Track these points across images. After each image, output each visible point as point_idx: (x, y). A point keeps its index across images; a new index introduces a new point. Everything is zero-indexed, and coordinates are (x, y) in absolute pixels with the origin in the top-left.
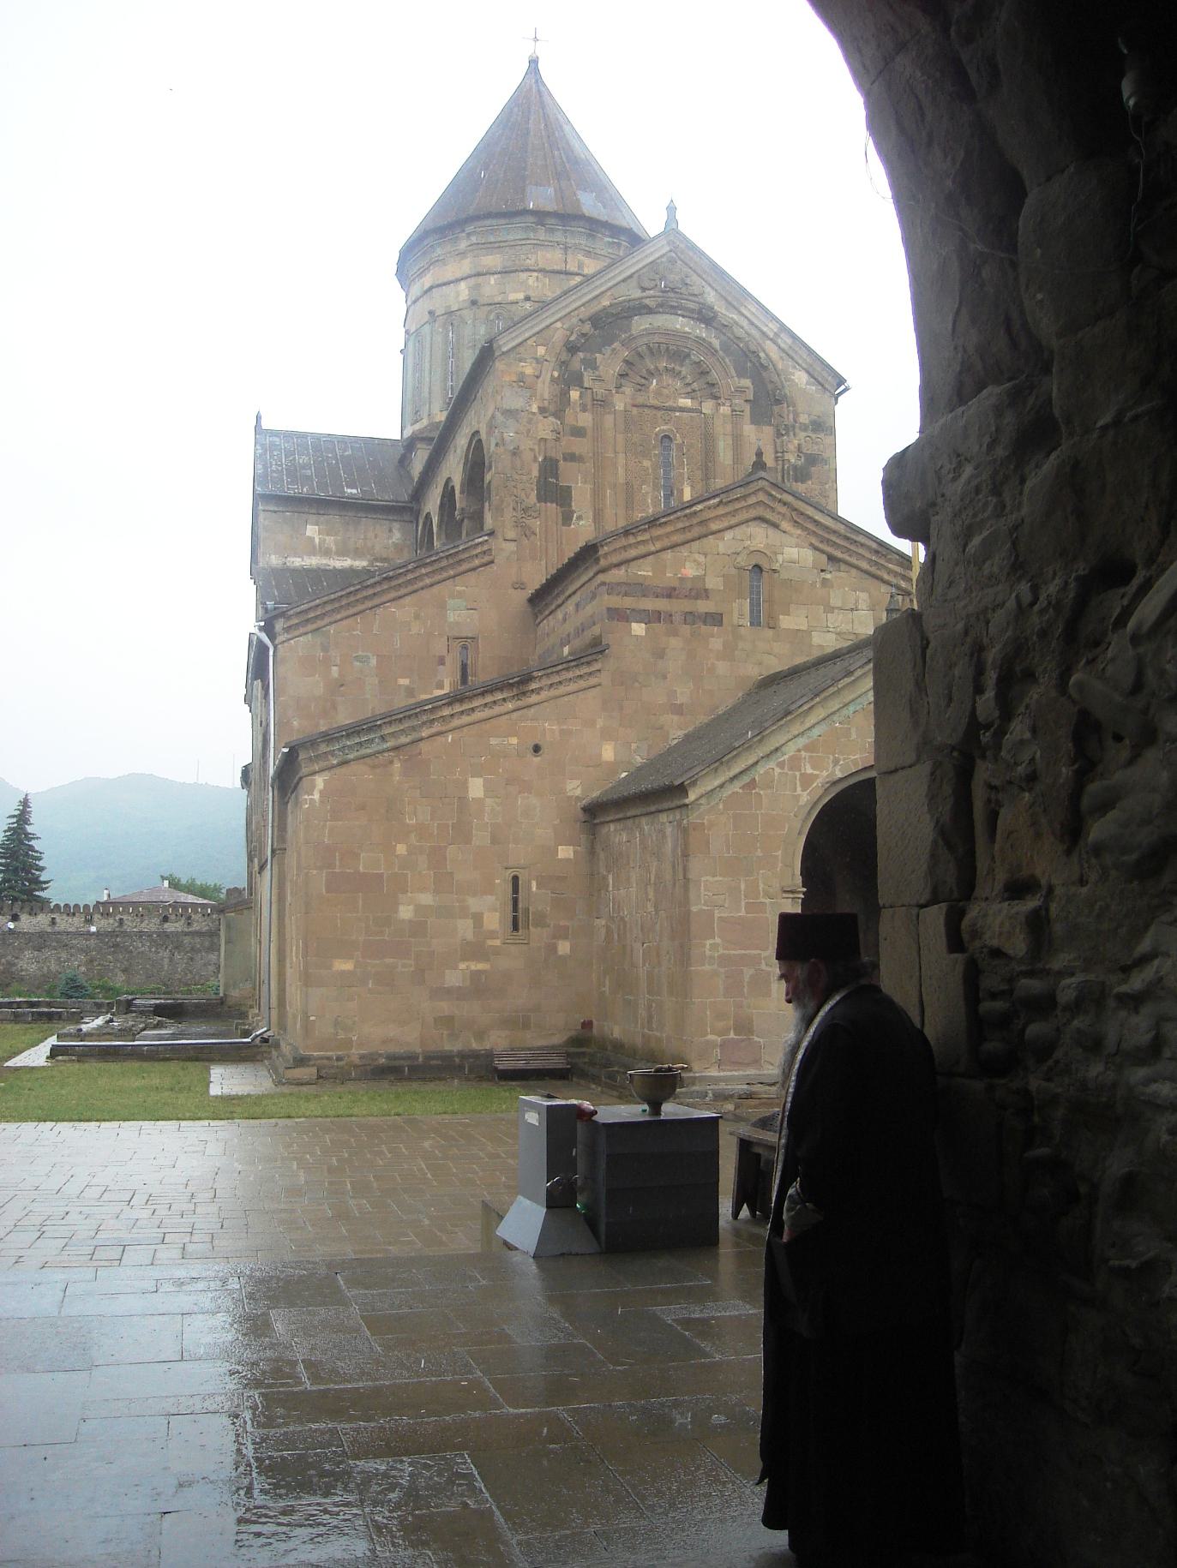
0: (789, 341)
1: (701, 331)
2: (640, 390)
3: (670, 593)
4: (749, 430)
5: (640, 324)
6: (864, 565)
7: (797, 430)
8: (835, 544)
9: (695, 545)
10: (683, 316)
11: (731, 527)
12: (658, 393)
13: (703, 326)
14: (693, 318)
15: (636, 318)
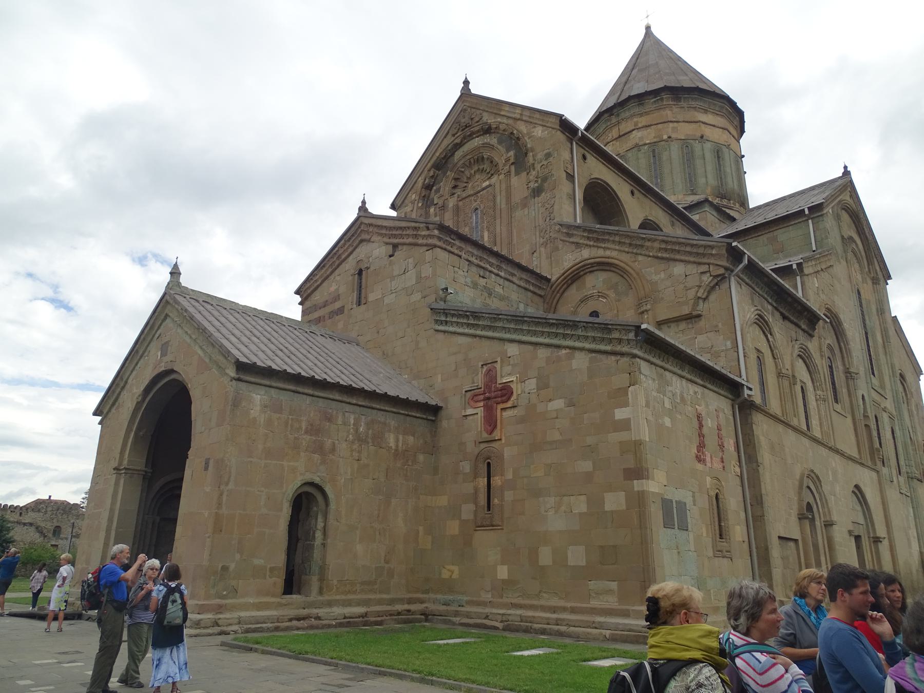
0: (527, 113)
1: (487, 139)
2: (464, 190)
3: (325, 305)
4: (515, 180)
5: (459, 154)
6: (410, 240)
7: (536, 165)
8: (395, 236)
9: (337, 272)
10: (478, 137)
11: (351, 253)
12: (473, 187)
13: (488, 135)
14: (480, 135)
15: (456, 153)
